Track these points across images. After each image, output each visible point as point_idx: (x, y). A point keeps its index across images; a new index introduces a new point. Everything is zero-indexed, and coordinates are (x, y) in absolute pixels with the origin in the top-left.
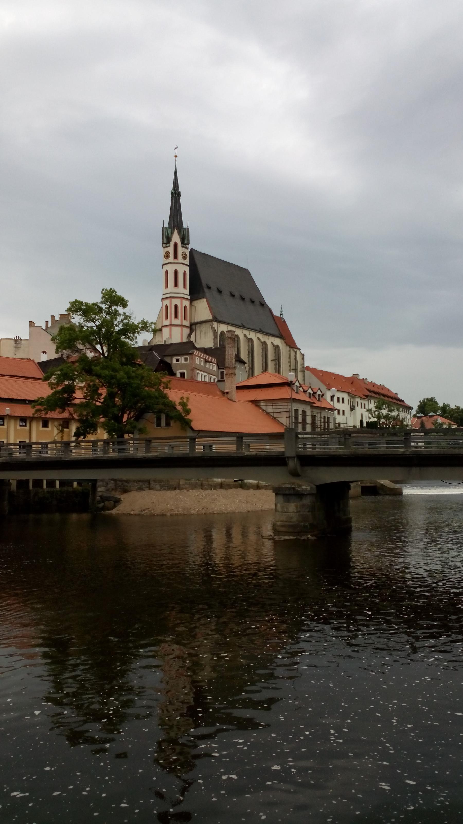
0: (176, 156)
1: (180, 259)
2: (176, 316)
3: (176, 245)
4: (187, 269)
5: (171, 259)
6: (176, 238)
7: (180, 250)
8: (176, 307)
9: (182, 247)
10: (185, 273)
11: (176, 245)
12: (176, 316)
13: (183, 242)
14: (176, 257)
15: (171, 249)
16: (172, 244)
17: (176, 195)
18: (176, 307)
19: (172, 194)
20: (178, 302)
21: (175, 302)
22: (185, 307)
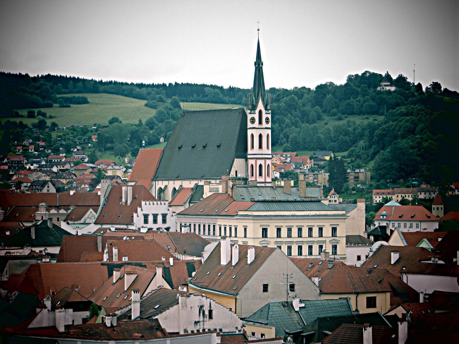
0: (258, 30)
1: (264, 125)
2: (261, 174)
3: (260, 112)
4: (269, 132)
5: (256, 124)
6: (260, 106)
7: (264, 116)
8: (261, 166)
9: (266, 113)
11: (260, 112)
12: (261, 174)
14: (260, 122)
16: (257, 111)
18: (261, 166)
19: (255, 64)
20: (262, 162)
21: (259, 162)
22: (268, 165)
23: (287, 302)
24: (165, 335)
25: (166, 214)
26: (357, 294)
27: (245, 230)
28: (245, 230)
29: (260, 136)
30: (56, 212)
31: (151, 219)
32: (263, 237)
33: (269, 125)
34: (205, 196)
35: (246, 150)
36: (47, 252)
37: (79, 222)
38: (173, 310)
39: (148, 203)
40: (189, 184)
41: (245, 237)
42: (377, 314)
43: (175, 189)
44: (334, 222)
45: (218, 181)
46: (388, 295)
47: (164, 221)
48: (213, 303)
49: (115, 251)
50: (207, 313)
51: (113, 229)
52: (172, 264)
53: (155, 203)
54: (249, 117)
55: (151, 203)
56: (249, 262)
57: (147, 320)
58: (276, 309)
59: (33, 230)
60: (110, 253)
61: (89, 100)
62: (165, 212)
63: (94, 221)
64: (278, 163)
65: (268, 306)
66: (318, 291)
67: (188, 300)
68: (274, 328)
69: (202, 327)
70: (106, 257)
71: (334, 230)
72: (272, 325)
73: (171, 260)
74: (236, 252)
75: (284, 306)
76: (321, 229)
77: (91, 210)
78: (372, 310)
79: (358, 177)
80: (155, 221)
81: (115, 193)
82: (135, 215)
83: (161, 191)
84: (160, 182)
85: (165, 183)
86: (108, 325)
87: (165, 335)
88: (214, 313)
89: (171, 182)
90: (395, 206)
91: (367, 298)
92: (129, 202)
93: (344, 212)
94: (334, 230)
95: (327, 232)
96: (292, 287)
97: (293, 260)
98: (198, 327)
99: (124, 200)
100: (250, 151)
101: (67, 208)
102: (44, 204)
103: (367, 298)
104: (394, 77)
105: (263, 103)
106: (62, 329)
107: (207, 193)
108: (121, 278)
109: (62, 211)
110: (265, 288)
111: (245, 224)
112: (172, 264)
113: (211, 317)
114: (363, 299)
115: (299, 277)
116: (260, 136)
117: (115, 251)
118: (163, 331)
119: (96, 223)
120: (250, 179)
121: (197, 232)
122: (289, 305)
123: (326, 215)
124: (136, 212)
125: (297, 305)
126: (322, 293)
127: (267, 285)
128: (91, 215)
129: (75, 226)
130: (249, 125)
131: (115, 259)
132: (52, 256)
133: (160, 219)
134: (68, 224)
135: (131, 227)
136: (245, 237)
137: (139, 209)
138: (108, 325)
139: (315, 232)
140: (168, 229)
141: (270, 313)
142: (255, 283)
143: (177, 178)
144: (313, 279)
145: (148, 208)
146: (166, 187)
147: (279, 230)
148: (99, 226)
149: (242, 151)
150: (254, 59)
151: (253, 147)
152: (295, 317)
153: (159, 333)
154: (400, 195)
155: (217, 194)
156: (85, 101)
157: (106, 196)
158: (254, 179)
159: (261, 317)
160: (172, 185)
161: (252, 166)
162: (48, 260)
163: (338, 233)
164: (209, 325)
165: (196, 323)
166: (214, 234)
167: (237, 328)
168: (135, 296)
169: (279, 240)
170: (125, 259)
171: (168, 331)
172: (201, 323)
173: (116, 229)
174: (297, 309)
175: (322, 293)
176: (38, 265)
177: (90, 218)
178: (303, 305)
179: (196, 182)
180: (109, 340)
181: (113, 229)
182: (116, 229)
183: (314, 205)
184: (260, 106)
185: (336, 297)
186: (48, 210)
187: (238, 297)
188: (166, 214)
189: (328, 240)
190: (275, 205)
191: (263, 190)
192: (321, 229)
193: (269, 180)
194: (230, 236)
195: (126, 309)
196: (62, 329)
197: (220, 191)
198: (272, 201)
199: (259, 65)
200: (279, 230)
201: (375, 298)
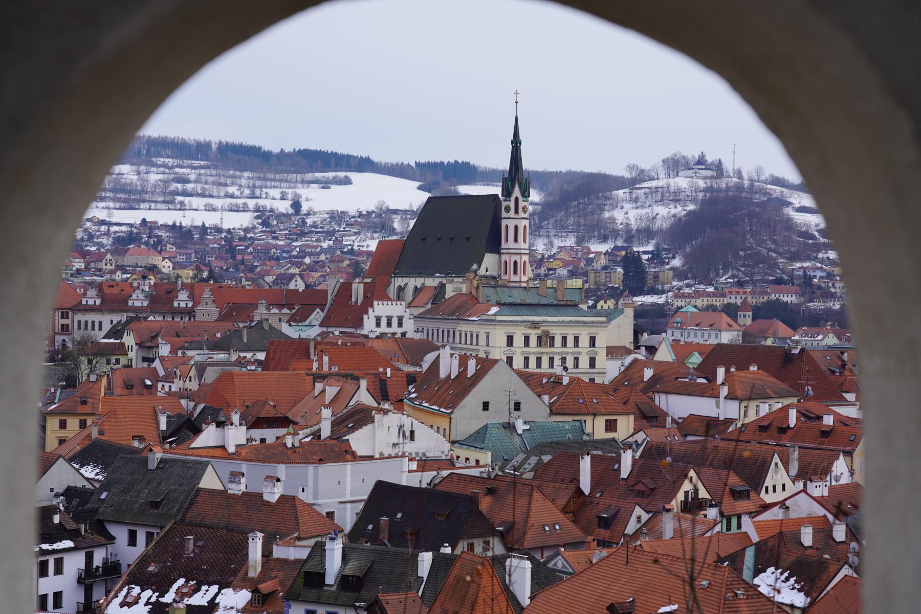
2: (515, 272)
3: (517, 199)
4: (527, 222)
5: (512, 214)
6: (517, 192)
7: (522, 204)
8: (515, 263)
10: (525, 227)
11: (517, 199)
13: (523, 196)
14: (516, 212)
15: (512, 204)
16: (513, 198)
18: (515, 263)
20: (517, 258)
21: (514, 258)
22: (525, 262)
23: (509, 423)
24: (355, 457)
25: (403, 317)
26: (595, 415)
27: (488, 337)
28: (488, 337)
29: (516, 228)
30: (277, 311)
31: (384, 322)
32: (508, 345)
33: (526, 215)
34: (447, 297)
35: (500, 244)
36: (255, 358)
37: (304, 323)
38: (366, 430)
39: (381, 303)
40: (432, 282)
41: (488, 345)
42: (614, 440)
43: (416, 287)
44: (593, 330)
45: (461, 280)
46: (632, 417)
47: (400, 324)
48: (416, 423)
49: (326, 359)
50: (408, 434)
51: (337, 333)
52: (389, 375)
53: (390, 303)
54: (504, 204)
55: (385, 303)
56: (469, 376)
57: (335, 441)
58: (494, 431)
59: (245, 332)
60: (320, 361)
61: (353, 180)
62: (402, 314)
63: (318, 323)
64: (567, 258)
65: (485, 428)
66: (548, 411)
67: (386, 418)
68: (489, 454)
69: (401, 450)
70: (315, 365)
71: (593, 342)
72: (488, 449)
73: (389, 370)
74: (456, 362)
75: (504, 428)
76: (577, 339)
77: (318, 310)
78: (610, 435)
79: (658, 277)
80: (389, 324)
81: (345, 289)
82: (365, 317)
83: (401, 289)
84: (400, 279)
85: (406, 280)
86: (289, 445)
87: (355, 457)
88: (416, 434)
89: (412, 280)
90: (692, 312)
91: (607, 421)
92: (359, 302)
93: (605, 319)
94: (593, 342)
95: (584, 341)
96: (517, 406)
97: (519, 373)
98: (396, 450)
99: (353, 299)
100: (503, 245)
101: (290, 306)
102: (264, 302)
103: (607, 421)
104: (710, 159)
105: (520, 190)
106: (231, 449)
107: (450, 292)
108: (324, 391)
109: (285, 311)
110: (486, 406)
111: (488, 331)
112: (389, 375)
113: (412, 438)
114: (600, 422)
115: (524, 393)
116: (516, 228)
117: (326, 359)
118: (353, 454)
119: (321, 325)
120: (503, 277)
121: (430, 339)
122: (510, 427)
123: (584, 322)
124: (367, 313)
125: (520, 427)
126: (552, 413)
127: (488, 403)
128: (317, 315)
129: (298, 328)
130: (504, 214)
131: (326, 368)
132: (259, 363)
133: (395, 322)
134: (290, 325)
135: (359, 331)
136: (488, 345)
137: (370, 310)
138: (289, 445)
139: (570, 341)
140: (404, 334)
141: (488, 435)
142: (473, 399)
143: (420, 275)
144: (543, 396)
145: (381, 309)
146: (406, 284)
147: (527, 339)
148: (325, 329)
149: (495, 245)
150: (511, 137)
151: (507, 240)
152: (517, 440)
153: (349, 457)
154: (705, 299)
155: (460, 295)
156: (347, 182)
157: (334, 294)
158: (507, 277)
159: (477, 439)
160: (413, 282)
161: (506, 262)
162: (253, 368)
163: (598, 343)
164: (410, 448)
165: (394, 445)
166: (454, 341)
167: (443, 452)
168: (326, 413)
169: (527, 349)
170: (335, 369)
171: (359, 453)
172: (401, 446)
173: (340, 333)
174: (520, 432)
175: (552, 413)
176: (231, 375)
177: (317, 320)
178: (527, 427)
179: (441, 280)
180: (278, 463)
181: (337, 333)
182: (340, 333)
183: (570, 310)
184: (517, 192)
185: (569, 419)
186: (268, 309)
187: (452, 416)
188: (403, 317)
189: (584, 351)
190: (524, 310)
191: (514, 291)
192: (577, 339)
193: (524, 279)
194: (471, 344)
195: (316, 428)
196: (231, 449)
197: (464, 292)
198: (520, 305)
199: (516, 144)
200: (527, 339)
201: (616, 421)
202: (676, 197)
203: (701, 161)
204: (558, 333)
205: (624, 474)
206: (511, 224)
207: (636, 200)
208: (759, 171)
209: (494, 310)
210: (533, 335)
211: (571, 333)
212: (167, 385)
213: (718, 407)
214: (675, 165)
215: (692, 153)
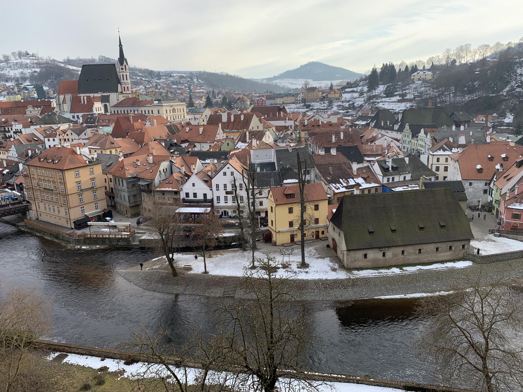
5: (124, 70)
17: (120, 45)
21: (127, 85)
92: (86, 103)
100: (122, 81)
104: (31, 53)
109: (39, 109)
121: (144, 113)
143: (91, 93)
149: (119, 82)
202: (26, 66)
203: (28, 54)
204: (176, 108)
205: (342, 138)
206: (125, 74)
207: (10, 67)
208: (49, 57)
209: (156, 102)
210: (171, 109)
211: (179, 107)
212: (51, 139)
213: (286, 122)
214: (20, 55)
215: (23, 51)
